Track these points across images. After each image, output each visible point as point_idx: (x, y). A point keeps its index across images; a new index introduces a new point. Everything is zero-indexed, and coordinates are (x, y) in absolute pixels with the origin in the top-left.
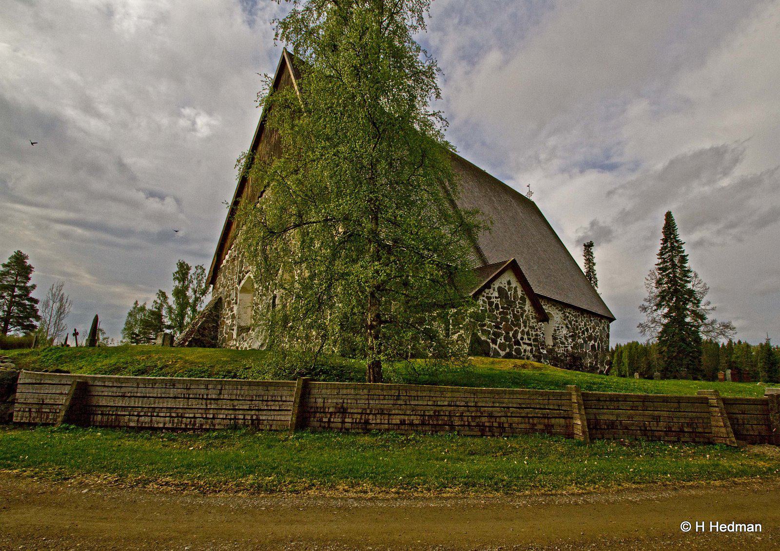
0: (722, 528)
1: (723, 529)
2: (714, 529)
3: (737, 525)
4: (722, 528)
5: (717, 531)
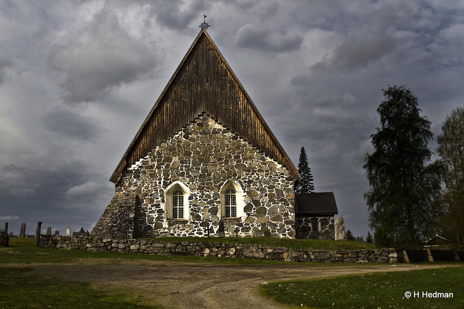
0: (429, 295)
1: (430, 296)
2: (425, 296)
3: (438, 294)
4: (429, 295)
5: (427, 297)
